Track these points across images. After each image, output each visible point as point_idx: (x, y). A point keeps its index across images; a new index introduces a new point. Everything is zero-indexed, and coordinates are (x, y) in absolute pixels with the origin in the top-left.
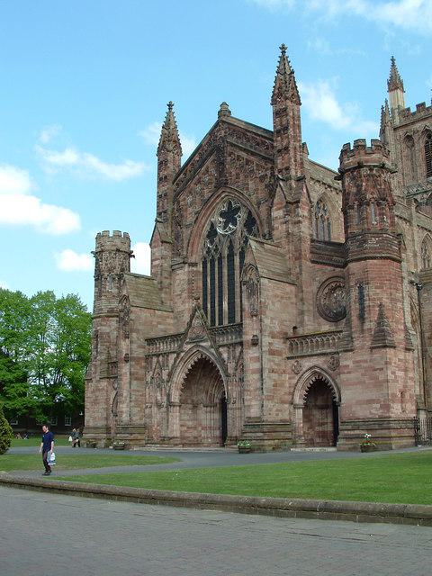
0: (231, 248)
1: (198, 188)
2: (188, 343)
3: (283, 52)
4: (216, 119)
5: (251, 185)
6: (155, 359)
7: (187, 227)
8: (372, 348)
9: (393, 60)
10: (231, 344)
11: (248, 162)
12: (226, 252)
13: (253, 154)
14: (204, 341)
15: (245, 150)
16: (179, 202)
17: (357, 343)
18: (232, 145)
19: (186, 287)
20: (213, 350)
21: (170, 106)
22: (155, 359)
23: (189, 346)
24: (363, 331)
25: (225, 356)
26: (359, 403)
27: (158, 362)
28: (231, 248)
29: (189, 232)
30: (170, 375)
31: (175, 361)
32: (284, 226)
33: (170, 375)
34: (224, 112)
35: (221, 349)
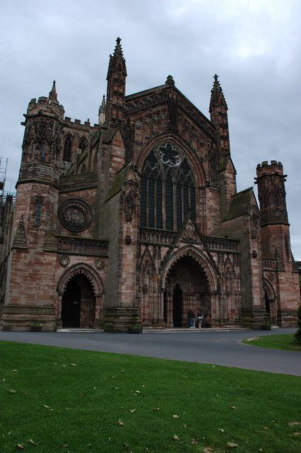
0: (169, 176)
1: (148, 120)
2: (182, 242)
3: (216, 79)
4: (162, 82)
5: (194, 145)
6: (143, 248)
8: (293, 272)
9: (54, 82)
10: (221, 252)
11: (193, 128)
12: (164, 177)
13: (198, 126)
14: (198, 244)
15: (192, 119)
16: (129, 120)
17: (286, 268)
18: (182, 109)
20: (205, 253)
21: (118, 40)
22: (143, 248)
23: (182, 245)
24: (288, 262)
25: (215, 259)
26: (289, 301)
27: (147, 250)
28: (169, 176)
29: (139, 149)
30: (163, 264)
31: (168, 253)
32: (233, 185)
33: (163, 264)
34: (170, 80)
35: (211, 253)
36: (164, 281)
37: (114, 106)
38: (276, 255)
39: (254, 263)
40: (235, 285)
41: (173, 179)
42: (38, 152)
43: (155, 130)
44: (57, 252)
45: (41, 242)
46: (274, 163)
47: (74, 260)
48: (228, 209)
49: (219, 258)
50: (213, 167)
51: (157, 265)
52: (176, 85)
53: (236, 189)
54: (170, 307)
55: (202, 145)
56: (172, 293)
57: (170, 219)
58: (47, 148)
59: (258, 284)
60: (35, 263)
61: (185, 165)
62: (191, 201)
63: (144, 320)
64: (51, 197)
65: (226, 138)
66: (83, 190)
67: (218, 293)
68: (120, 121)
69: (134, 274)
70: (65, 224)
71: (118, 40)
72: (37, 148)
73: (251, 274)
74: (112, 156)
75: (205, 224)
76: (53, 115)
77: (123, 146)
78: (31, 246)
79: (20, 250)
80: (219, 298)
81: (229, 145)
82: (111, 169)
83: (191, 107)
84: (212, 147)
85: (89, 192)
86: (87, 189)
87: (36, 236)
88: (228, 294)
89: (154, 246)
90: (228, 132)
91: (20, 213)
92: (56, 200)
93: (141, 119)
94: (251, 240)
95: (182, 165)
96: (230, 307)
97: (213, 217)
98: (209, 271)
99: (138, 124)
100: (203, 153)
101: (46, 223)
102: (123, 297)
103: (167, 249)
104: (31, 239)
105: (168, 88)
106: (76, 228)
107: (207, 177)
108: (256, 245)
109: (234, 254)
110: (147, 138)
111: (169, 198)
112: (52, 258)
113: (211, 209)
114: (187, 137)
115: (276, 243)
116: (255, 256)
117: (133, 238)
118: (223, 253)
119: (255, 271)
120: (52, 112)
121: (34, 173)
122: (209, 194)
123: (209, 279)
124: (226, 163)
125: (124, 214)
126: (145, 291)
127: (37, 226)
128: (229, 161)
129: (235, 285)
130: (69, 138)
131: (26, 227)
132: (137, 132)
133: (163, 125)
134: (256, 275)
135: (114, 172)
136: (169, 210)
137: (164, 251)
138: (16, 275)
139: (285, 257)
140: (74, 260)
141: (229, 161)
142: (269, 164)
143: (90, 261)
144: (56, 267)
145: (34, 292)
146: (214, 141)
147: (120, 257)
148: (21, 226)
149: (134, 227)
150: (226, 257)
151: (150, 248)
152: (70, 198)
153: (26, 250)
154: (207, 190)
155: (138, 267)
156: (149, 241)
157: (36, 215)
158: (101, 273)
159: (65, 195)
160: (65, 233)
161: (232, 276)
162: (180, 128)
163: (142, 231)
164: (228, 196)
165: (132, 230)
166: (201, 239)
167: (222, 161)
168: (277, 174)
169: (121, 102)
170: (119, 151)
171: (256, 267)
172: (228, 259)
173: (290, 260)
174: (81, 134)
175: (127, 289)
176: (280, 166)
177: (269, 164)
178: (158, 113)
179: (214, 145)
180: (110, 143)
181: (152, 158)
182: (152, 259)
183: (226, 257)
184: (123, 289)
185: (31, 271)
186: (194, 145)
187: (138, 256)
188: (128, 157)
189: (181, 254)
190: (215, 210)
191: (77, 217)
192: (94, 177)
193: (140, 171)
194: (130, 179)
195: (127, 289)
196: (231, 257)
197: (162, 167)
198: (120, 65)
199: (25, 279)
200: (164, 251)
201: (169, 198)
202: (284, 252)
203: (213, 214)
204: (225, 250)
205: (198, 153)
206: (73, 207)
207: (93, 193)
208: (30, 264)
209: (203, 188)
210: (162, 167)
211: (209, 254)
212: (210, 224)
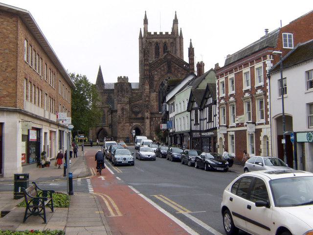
19: (155, 98)
47: (134, 124)
55: (183, 74)
70: (133, 112)
74: (145, 90)
99: (156, 73)
104: (121, 120)
106: (136, 113)
112: (128, 124)
114: (176, 72)
117: (149, 117)
121: (121, 101)
133: (166, 71)
140: (134, 124)
143: (139, 124)
144: (129, 126)
157: (123, 113)
158: (143, 127)
160: (133, 116)
174: (164, 40)
178: (163, 66)
191: (137, 109)
207: (141, 101)
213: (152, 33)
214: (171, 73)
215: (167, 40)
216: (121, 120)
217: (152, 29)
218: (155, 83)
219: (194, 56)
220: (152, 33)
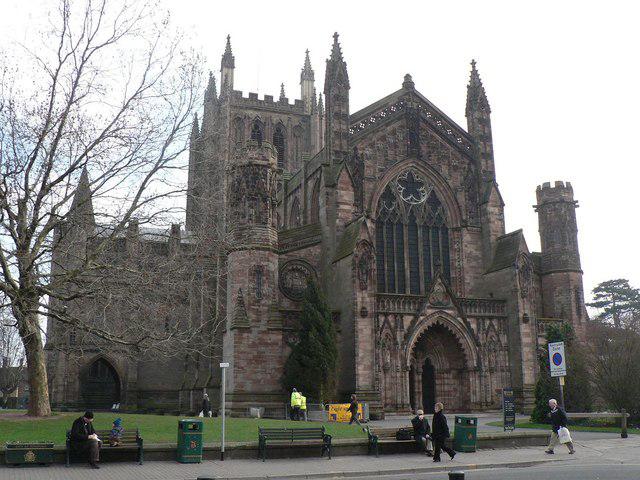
0: (412, 218)
1: (380, 144)
3: (474, 67)
4: (397, 86)
5: (444, 170)
7: (369, 179)
9: (229, 38)
12: (406, 221)
15: (441, 134)
16: (356, 149)
23: (430, 311)
24: (580, 324)
25: (473, 326)
27: (386, 321)
28: (412, 218)
29: (371, 186)
33: (407, 337)
34: (408, 83)
36: (409, 357)
37: (337, 134)
38: (563, 315)
39: (524, 329)
40: (501, 358)
41: (417, 221)
42: (252, 211)
43: (390, 158)
44: (284, 330)
45: (264, 319)
46: (559, 184)
48: (492, 257)
49: (478, 325)
50: (472, 198)
51: (399, 338)
52: (417, 87)
53: (504, 231)
54: (419, 387)
55: (456, 168)
56: (421, 370)
57: (415, 275)
58: (262, 204)
59: (530, 356)
60: (260, 343)
61: (434, 200)
62: (443, 247)
63: (386, 405)
64: (271, 265)
65: (489, 156)
66: (303, 248)
67: (478, 369)
68: (345, 153)
69: (372, 351)
71: (336, 36)
72: (251, 206)
73: (520, 344)
74: (338, 204)
75: (462, 279)
76: (265, 163)
77: (351, 188)
78: (254, 324)
79: (242, 330)
80: (480, 376)
81: (493, 166)
82: (337, 221)
83: (439, 115)
84: (470, 169)
85: (312, 249)
86: (309, 246)
87: (258, 312)
88: (491, 371)
89: (395, 315)
90: (491, 147)
91: (238, 286)
92: (276, 266)
93: (372, 146)
94: (520, 301)
95: (428, 201)
96: (495, 387)
97: (472, 267)
98: (466, 341)
99: (368, 152)
100: (456, 180)
101: (268, 297)
102: (361, 379)
103: (411, 318)
104: (252, 316)
105: (406, 94)
107: (464, 213)
108: (527, 306)
109: (499, 318)
110: (382, 170)
111: (414, 246)
113: (469, 256)
115: (562, 298)
116: (526, 320)
118: (483, 318)
119: (525, 340)
120: (265, 159)
122: (467, 237)
123: (467, 352)
124: (488, 192)
125: (357, 281)
126: (386, 371)
127: (258, 301)
128: (493, 189)
129: (501, 358)
130: (256, 127)
131: (246, 302)
132: (368, 163)
133: (402, 149)
134: (527, 345)
135: (342, 224)
136: (414, 261)
137: (408, 320)
138: (239, 358)
139: (575, 316)
141: (493, 189)
142: (553, 186)
145: (259, 376)
146: (473, 161)
147: (353, 331)
148: (241, 302)
149: (370, 296)
150: (488, 322)
151: (390, 318)
152: (290, 259)
153: (248, 330)
154: (464, 231)
155: (377, 343)
156: (389, 309)
159: (283, 256)
161: (497, 348)
162: (424, 149)
163: (379, 298)
164: (493, 238)
165: (368, 299)
166: (454, 302)
167: (483, 190)
168: (562, 201)
169: (345, 127)
170: (347, 195)
171: (527, 335)
172: (491, 325)
173: (583, 320)
174: (276, 118)
175: (365, 369)
176: (569, 189)
177: (553, 186)
178: (394, 133)
179: (473, 167)
180: (334, 186)
181: (389, 195)
182: (394, 331)
183: (488, 322)
184: (361, 370)
185: (256, 354)
186: (444, 170)
187: (376, 330)
188: (359, 200)
189: (429, 323)
190: (476, 258)
192: (316, 228)
193: (373, 216)
194: (362, 238)
195: (365, 369)
196: (495, 322)
197: (402, 206)
198: (340, 75)
199: (250, 362)
200: (408, 320)
201: (414, 246)
202: (574, 309)
203: (474, 264)
204: (487, 314)
205: (450, 182)
206: (293, 270)
207: (316, 251)
208: (254, 345)
209: (457, 229)
210: (402, 206)
211: (465, 321)
212: (468, 279)
213: (246, 95)
214: (419, 157)
215: (284, 118)
216: (252, 316)
217: (245, 83)
218: (368, 186)
219: (488, 111)
220: (246, 95)
